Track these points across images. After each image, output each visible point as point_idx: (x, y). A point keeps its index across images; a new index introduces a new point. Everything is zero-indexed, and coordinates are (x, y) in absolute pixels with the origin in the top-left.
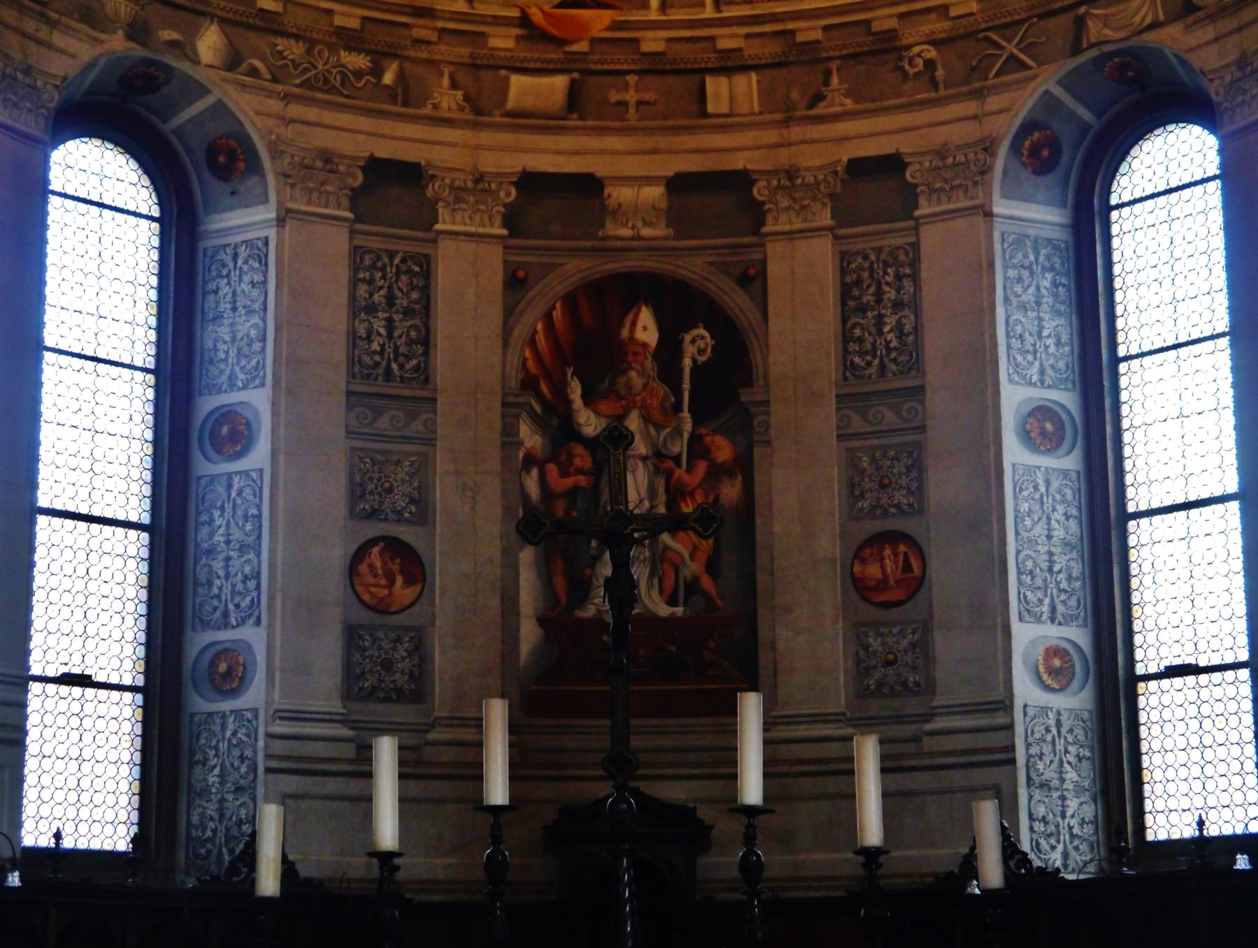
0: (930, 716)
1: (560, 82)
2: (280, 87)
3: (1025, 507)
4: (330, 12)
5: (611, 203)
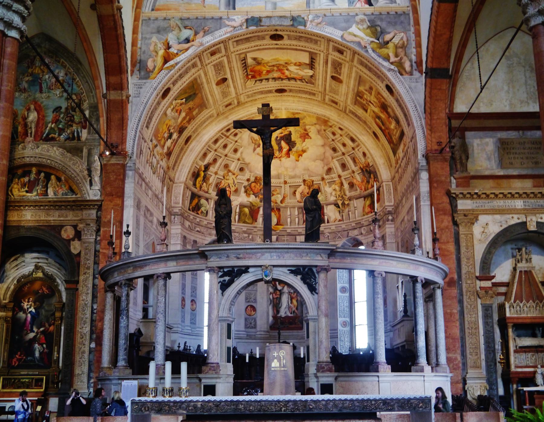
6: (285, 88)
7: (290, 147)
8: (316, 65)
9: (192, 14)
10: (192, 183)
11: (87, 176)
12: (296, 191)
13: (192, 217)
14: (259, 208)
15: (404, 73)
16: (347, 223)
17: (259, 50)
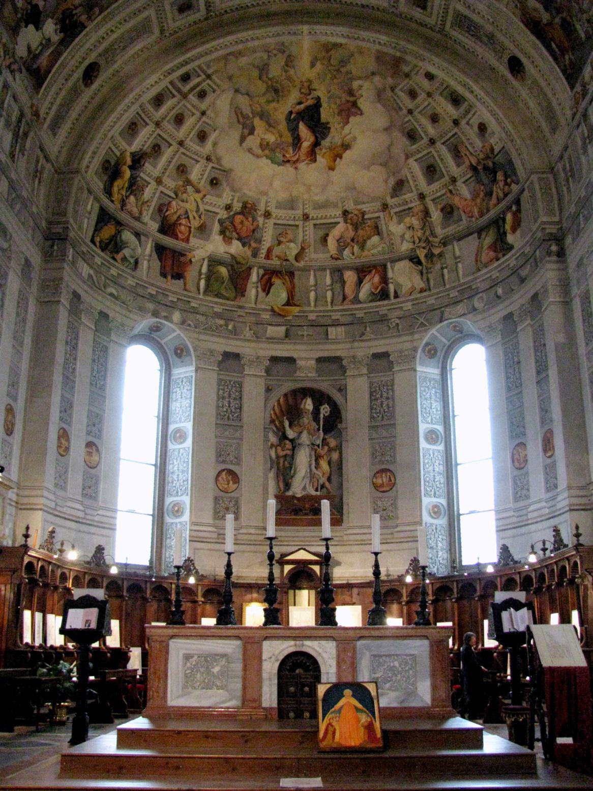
0: (397, 526)
1: (283, 329)
2: (197, 330)
3: (426, 461)
4: (213, 307)
5: (298, 366)
7: (316, 137)
10: (102, 186)
12: (327, 235)
13: (98, 260)
14: (250, 268)
16: (438, 293)
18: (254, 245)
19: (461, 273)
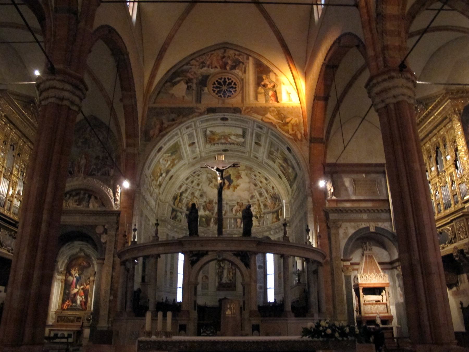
6: (228, 149)
8: (246, 136)
9: (177, 105)
11: (112, 197)
13: (172, 223)
14: (211, 218)
15: (297, 140)
17: (214, 126)
18: (212, 212)
19: (268, 222)
